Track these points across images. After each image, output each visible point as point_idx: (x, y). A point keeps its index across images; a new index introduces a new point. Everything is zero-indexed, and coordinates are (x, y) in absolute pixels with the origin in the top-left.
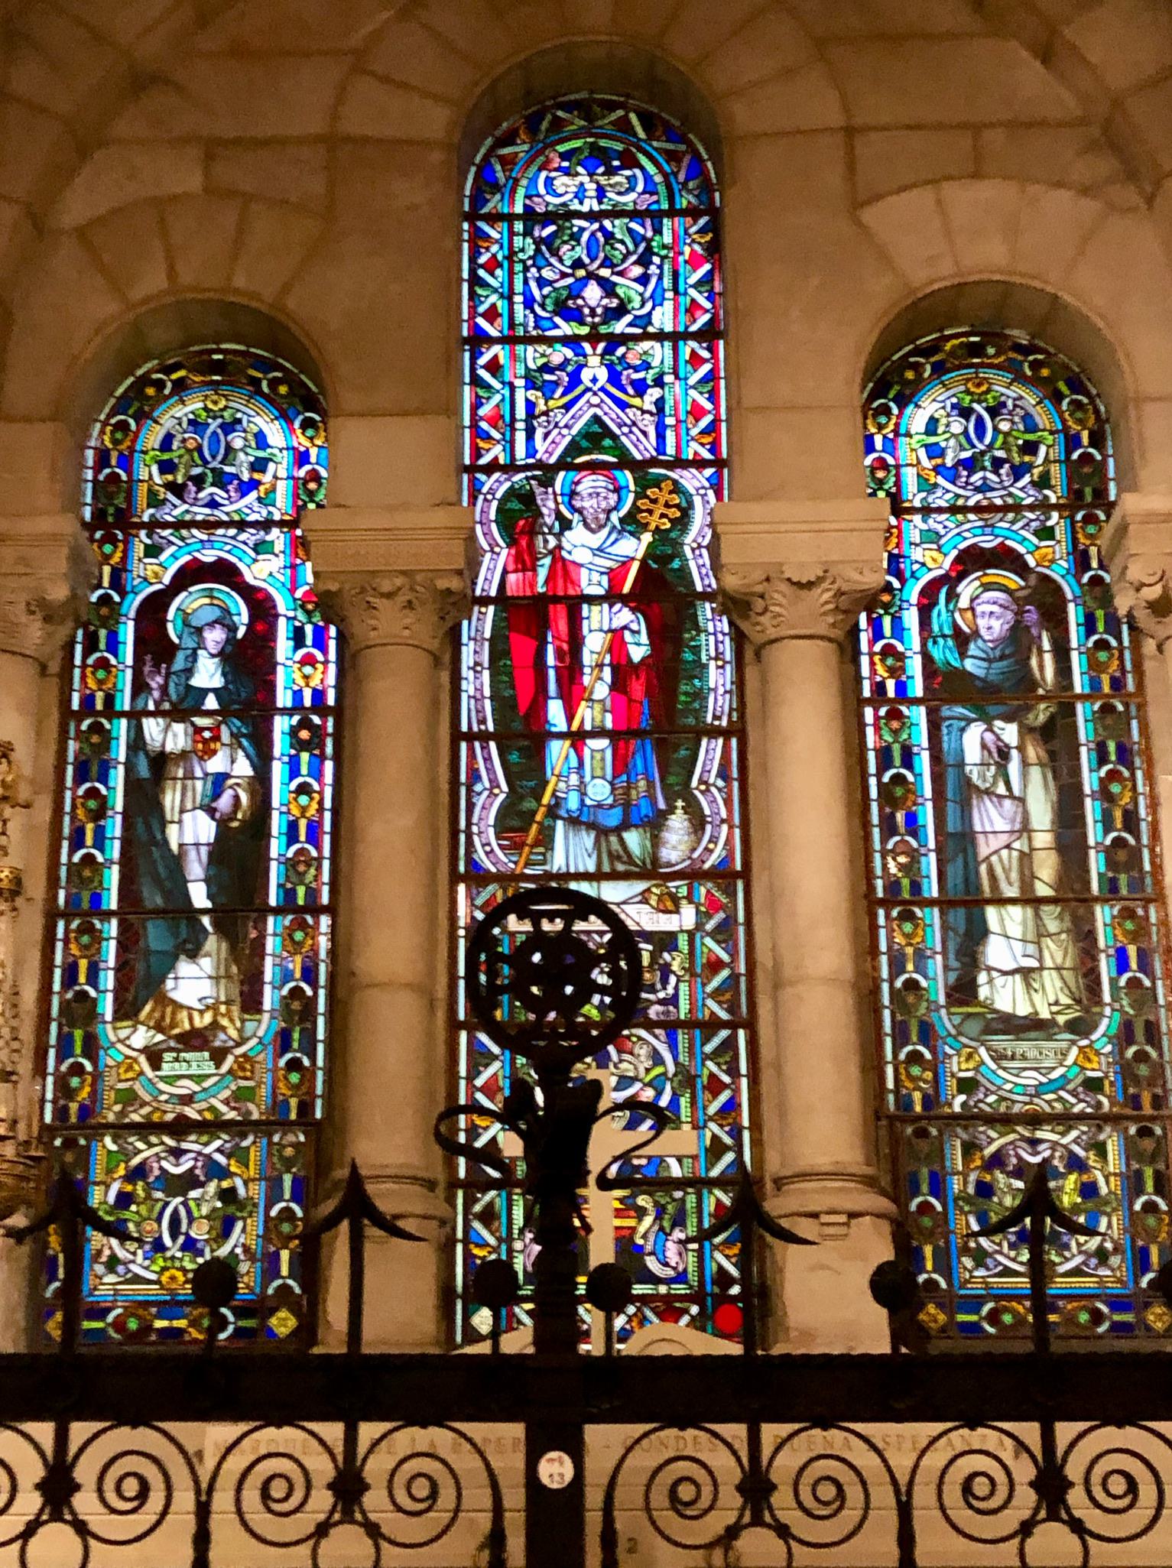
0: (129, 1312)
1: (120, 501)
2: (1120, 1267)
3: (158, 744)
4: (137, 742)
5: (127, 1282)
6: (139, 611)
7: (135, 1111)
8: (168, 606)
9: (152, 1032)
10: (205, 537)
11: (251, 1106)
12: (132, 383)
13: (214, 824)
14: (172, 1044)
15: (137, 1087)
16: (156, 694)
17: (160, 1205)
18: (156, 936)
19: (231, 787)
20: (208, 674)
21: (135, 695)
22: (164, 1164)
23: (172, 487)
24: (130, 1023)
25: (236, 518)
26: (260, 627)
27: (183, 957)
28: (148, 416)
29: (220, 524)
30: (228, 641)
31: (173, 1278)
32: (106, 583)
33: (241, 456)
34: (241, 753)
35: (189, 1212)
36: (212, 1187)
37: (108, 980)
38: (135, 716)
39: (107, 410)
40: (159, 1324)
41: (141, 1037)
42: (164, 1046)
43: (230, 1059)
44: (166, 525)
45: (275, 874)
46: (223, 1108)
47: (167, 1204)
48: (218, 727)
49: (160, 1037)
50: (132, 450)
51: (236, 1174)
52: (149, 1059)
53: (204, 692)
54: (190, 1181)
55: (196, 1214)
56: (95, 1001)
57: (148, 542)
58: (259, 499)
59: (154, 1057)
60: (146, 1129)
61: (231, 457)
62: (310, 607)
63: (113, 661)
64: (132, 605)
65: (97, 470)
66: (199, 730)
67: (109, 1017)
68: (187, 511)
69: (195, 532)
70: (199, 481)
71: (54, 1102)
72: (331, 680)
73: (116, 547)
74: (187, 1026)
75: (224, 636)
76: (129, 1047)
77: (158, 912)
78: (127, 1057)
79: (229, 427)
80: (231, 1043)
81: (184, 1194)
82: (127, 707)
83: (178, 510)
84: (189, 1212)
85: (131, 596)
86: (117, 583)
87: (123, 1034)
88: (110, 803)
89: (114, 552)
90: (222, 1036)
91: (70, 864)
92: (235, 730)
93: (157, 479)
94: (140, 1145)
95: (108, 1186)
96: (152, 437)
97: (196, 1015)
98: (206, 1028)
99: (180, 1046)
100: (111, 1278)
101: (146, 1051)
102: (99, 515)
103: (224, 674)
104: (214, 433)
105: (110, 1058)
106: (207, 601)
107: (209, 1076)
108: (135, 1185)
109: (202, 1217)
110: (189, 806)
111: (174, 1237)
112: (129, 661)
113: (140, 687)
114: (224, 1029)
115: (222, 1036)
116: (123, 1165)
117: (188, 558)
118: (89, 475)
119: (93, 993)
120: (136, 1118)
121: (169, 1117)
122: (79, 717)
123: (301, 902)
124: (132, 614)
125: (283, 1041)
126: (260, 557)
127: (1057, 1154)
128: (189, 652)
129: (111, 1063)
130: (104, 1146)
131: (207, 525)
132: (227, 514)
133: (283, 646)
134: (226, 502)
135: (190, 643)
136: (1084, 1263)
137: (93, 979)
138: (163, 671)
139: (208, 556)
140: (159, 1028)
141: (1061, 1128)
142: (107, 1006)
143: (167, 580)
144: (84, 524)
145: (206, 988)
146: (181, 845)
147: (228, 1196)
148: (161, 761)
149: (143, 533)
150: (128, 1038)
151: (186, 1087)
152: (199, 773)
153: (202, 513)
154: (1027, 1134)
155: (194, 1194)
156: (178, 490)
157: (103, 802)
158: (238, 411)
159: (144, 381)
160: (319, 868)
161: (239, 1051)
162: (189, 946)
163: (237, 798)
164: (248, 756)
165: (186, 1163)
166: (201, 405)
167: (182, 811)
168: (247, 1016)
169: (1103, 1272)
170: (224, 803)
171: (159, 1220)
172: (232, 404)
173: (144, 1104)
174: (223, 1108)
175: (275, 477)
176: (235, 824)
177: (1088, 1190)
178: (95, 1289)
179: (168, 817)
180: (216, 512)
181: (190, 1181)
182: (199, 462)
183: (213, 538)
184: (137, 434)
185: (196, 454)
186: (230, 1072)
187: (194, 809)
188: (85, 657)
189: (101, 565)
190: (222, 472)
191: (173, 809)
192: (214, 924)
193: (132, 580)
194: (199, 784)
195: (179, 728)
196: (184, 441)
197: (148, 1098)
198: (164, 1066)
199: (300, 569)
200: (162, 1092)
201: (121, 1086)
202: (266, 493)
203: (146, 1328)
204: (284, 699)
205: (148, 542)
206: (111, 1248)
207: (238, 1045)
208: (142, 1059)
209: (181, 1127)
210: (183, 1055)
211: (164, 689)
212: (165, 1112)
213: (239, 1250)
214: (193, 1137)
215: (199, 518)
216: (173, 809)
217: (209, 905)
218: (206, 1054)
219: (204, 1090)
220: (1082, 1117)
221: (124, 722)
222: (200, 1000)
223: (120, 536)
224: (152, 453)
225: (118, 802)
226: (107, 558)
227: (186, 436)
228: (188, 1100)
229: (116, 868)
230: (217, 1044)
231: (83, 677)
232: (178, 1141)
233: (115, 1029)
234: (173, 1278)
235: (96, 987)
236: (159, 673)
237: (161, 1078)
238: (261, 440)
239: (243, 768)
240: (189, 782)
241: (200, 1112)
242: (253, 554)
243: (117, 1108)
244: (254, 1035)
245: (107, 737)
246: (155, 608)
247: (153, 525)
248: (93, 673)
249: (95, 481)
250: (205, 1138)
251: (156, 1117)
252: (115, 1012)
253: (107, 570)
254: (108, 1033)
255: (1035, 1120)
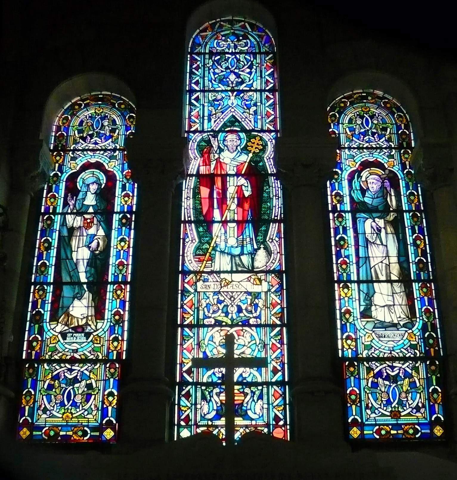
0: (50, 429)
1: (63, 142)
2: (424, 412)
3: (71, 224)
4: (64, 223)
5: (49, 417)
6: (67, 179)
7: (56, 355)
8: (78, 176)
9: (63, 326)
10: (92, 154)
11: (99, 354)
12: (70, 105)
13: (89, 252)
14: (71, 330)
15: (57, 346)
16: (71, 207)
17: (64, 389)
18: (67, 291)
19: (96, 239)
20: (90, 200)
21: (63, 208)
22: (66, 374)
23: (81, 138)
24: (56, 323)
25: (104, 148)
26: (110, 184)
27: (76, 299)
28: (75, 115)
29: (98, 150)
30: (98, 189)
31: (67, 416)
32: (56, 170)
33: (107, 128)
34: (100, 227)
35: (74, 391)
36: (83, 383)
37: (48, 307)
38: (64, 214)
39: (61, 113)
40: (62, 433)
41: (60, 328)
42: (67, 331)
43: (92, 336)
44: (79, 150)
45: (111, 270)
46: (89, 354)
47: (66, 389)
48: (93, 218)
49: (66, 328)
50: (69, 126)
51: (92, 378)
52: (62, 336)
53: (88, 206)
54: (75, 380)
55: (77, 393)
56: (43, 314)
57: (72, 156)
58: (112, 142)
59: (64, 335)
60: (60, 361)
61: (103, 128)
62: (128, 177)
63: (57, 196)
64: (65, 177)
65: (56, 132)
66: (85, 219)
67: (48, 321)
68: (87, 146)
69: (89, 152)
70: (91, 136)
71: (27, 351)
72: (135, 202)
73: (61, 158)
74: (76, 325)
75: (97, 187)
76: (55, 331)
77: (67, 283)
78: (54, 335)
79: (104, 118)
80: (92, 331)
81: (73, 385)
82: (61, 212)
83: (82, 145)
84: (74, 391)
85: (65, 174)
86: (60, 170)
87: (52, 327)
88: (53, 245)
89: (60, 159)
90: (89, 328)
91: (37, 266)
92: (99, 219)
93: (77, 135)
94: (57, 367)
95: (45, 382)
96: (76, 122)
97: (80, 320)
98: (83, 325)
99: (73, 331)
100: (44, 416)
101: (60, 333)
102: (56, 147)
103: (96, 200)
104: (98, 120)
105: (48, 335)
106: (92, 175)
107: (84, 342)
108: (55, 381)
109: (79, 394)
110: (81, 245)
111: (68, 402)
112: (63, 196)
113: (66, 204)
114: (90, 325)
115: (89, 328)
116: (51, 374)
117: (86, 161)
118: (53, 134)
119: (43, 312)
120: (56, 357)
121: (68, 357)
122: (44, 214)
123: (120, 280)
124: (65, 180)
125: (112, 330)
126: (111, 161)
127: (401, 372)
128: (84, 192)
129: (48, 337)
130: (44, 367)
131: (93, 150)
132: (101, 147)
133: (118, 191)
134: (101, 143)
135: (85, 189)
136: (411, 411)
137: (43, 307)
138: (74, 199)
139: (93, 161)
140: (66, 325)
141: (402, 362)
142: (47, 316)
143: (78, 169)
144: (51, 150)
145: (84, 311)
146: (77, 259)
147: (89, 386)
148: (71, 230)
149: (71, 153)
150: (55, 328)
151: (75, 346)
152: (85, 234)
153: (92, 146)
154: (390, 364)
155: (77, 385)
156: (84, 139)
157: (50, 244)
158: (106, 113)
159: (75, 103)
160: (127, 268)
161: (95, 334)
162: (78, 295)
163: (98, 243)
164: (103, 228)
165: (74, 374)
166: (94, 111)
167: (78, 248)
168: (98, 321)
169: (418, 414)
170: (94, 245)
171: (63, 395)
172: (104, 111)
173: (59, 352)
174: (89, 354)
175: (118, 134)
176: (97, 252)
177: (412, 385)
178: (38, 419)
179: (73, 250)
180: (97, 146)
181: (75, 380)
182: (92, 130)
183: (95, 154)
184: (71, 121)
185: (91, 127)
186: (91, 341)
187: (83, 247)
188: (47, 194)
189: (55, 163)
190: (100, 133)
191: (75, 246)
192: (87, 287)
193: (64, 169)
194: (85, 238)
195: (79, 218)
196: (87, 123)
197: (61, 350)
198: (67, 338)
199: (125, 164)
200: (66, 348)
201: (51, 345)
202: (115, 140)
203: (57, 434)
204: (117, 208)
205: (72, 156)
206: (45, 404)
207: (95, 331)
208: (59, 336)
209: (73, 361)
210: (74, 334)
211: (74, 206)
212: (67, 355)
213: (93, 407)
214: (77, 365)
215: (91, 148)
216: (75, 246)
217: (86, 281)
218: (83, 334)
219: (82, 347)
220: (410, 358)
221: (59, 216)
222: (82, 315)
223: (63, 154)
224: (75, 127)
225: (55, 243)
226: (57, 162)
227: (88, 121)
228: (76, 351)
229: (53, 267)
230: (87, 331)
231: (46, 201)
232: (72, 366)
233: (50, 325)
234: (67, 416)
235: (44, 309)
236: (73, 200)
237: (66, 343)
238: (114, 122)
239: (101, 232)
240: (82, 237)
241: (80, 356)
242: (109, 160)
243: (50, 353)
244: (101, 328)
245: (52, 221)
246: (73, 178)
247: (74, 150)
248: (50, 200)
249: (55, 136)
250: (81, 365)
251: (64, 357)
252: (50, 320)
253: (57, 165)
254: (46, 326)
255: (393, 359)
